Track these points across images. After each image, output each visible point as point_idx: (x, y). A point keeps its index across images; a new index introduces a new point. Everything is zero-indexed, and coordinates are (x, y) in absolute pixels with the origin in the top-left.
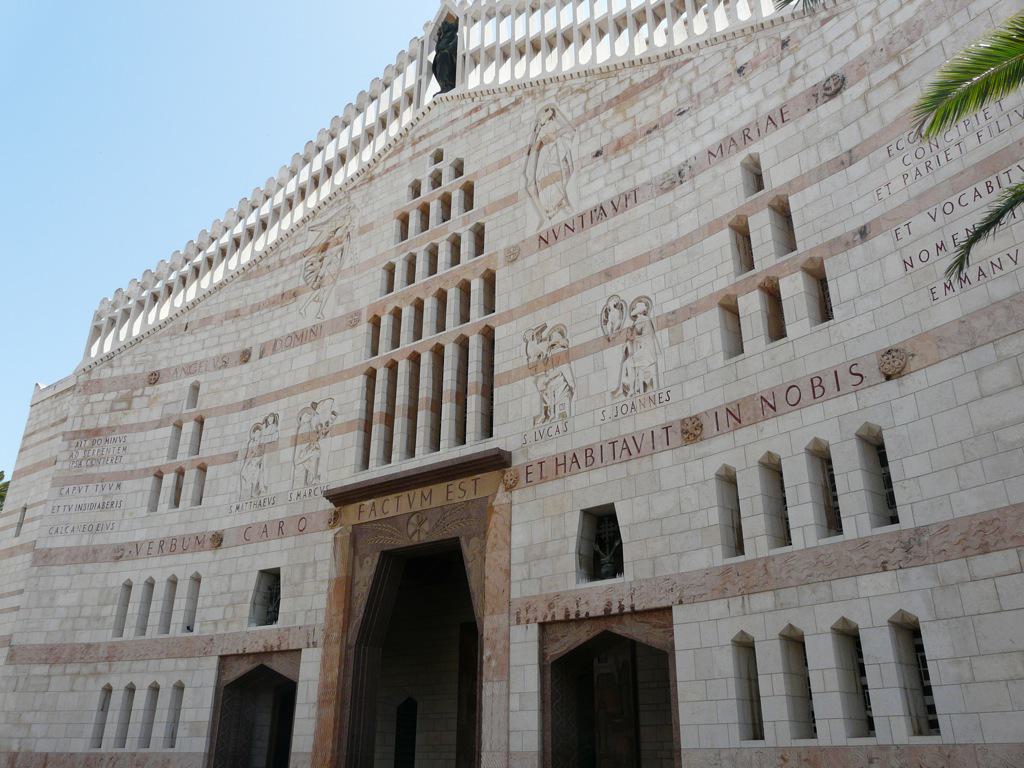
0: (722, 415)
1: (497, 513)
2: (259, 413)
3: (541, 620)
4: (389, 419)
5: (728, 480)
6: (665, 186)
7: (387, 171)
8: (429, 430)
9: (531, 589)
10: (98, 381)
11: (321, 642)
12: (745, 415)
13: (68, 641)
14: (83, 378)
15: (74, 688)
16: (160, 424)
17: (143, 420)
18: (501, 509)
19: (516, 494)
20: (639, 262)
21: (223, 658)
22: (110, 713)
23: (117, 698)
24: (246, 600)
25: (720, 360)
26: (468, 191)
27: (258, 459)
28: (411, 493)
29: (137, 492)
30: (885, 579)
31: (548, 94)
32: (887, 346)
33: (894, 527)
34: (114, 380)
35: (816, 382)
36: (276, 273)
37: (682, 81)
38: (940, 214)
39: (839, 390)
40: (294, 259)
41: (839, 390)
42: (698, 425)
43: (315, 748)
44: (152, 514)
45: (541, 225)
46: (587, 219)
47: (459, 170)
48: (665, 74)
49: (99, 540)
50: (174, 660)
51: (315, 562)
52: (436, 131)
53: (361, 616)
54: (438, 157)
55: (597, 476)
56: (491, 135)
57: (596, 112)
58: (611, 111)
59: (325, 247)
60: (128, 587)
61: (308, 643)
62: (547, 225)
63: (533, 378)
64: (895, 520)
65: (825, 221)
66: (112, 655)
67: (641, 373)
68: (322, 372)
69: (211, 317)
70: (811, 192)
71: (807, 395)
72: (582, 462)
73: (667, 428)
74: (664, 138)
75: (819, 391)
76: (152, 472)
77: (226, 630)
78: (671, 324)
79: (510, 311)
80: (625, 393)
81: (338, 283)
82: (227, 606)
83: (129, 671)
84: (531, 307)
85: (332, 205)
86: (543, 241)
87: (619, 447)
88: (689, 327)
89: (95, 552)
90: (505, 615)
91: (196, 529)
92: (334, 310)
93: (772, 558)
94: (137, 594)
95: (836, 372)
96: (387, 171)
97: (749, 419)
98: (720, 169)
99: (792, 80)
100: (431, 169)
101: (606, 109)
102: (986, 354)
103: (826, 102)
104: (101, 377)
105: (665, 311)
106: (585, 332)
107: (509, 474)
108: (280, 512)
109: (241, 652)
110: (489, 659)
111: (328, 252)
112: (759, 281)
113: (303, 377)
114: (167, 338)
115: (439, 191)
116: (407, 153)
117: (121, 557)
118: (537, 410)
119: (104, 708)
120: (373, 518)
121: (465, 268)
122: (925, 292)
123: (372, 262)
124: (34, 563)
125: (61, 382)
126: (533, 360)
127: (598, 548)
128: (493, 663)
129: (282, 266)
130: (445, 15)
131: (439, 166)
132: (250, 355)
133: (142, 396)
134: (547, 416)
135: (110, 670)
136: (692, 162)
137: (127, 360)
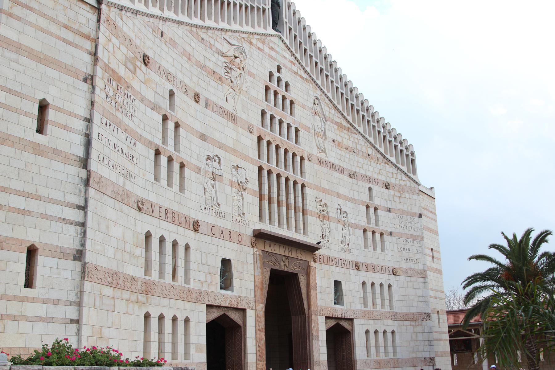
0: (364, 265)
3: (326, 315)
23: (154, 323)
24: (217, 272)
32: (395, 266)
38: (404, 241)
49: (129, 186)
52: (277, 52)
54: (279, 69)
58: (336, 127)
62: (319, 155)
86: (320, 161)
87: (342, 261)
91: (184, 211)
96: (259, 48)
98: (364, 184)
99: (379, 173)
102: (408, 279)
106: (333, 213)
128: (315, 328)
135: (147, 301)
136: (357, 174)
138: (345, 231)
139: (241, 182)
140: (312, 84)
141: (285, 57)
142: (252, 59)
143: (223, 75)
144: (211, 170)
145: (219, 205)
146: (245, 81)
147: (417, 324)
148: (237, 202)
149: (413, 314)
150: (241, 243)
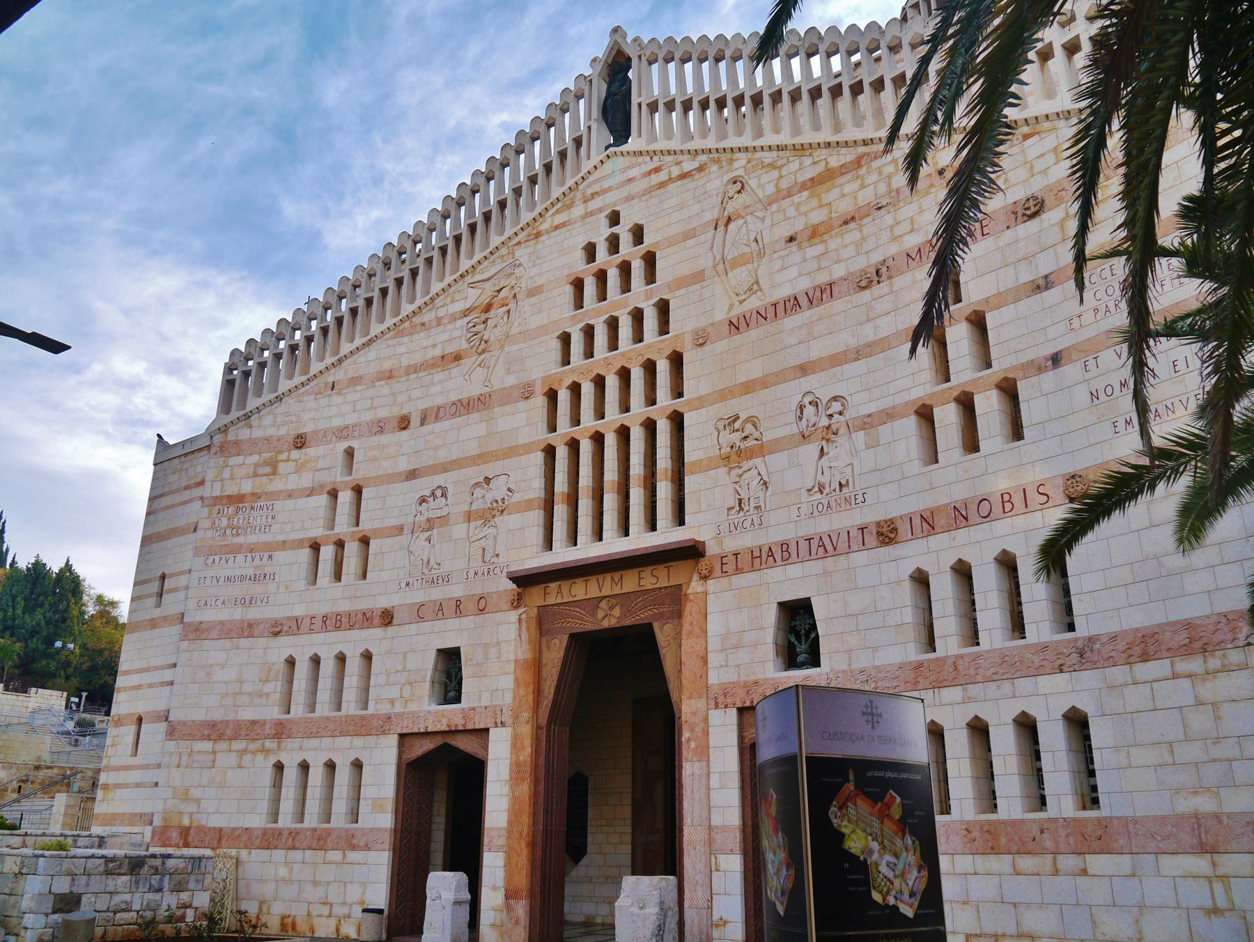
0: (917, 521)
1: (691, 601)
2: (425, 485)
4: (573, 500)
5: (921, 580)
6: (863, 284)
7: (557, 227)
8: (616, 514)
9: (729, 676)
10: (236, 443)
11: (509, 721)
12: (940, 522)
13: (231, 717)
14: (218, 438)
15: (243, 764)
16: (311, 492)
17: (291, 486)
18: (696, 598)
19: (710, 582)
20: (837, 360)
21: (402, 736)
22: (284, 790)
23: (291, 775)
25: (916, 467)
26: (650, 260)
27: (426, 534)
28: (598, 576)
29: (291, 564)
30: (1060, 679)
31: (736, 164)
33: (1070, 635)
34: (254, 442)
35: (1006, 497)
36: (433, 331)
37: (880, 173)
39: (1026, 507)
40: (454, 318)
41: (1026, 507)
42: (893, 529)
43: (510, 822)
44: (310, 588)
45: (731, 307)
46: (780, 308)
47: (638, 234)
48: (863, 164)
49: (253, 614)
50: (349, 738)
51: (499, 643)
53: (551, 696)
54: (614, 219)
55: (794, 570)
56: (673, 202)
57: (789, 194)
59: (488, 308)
60: (291, 662)
61: (496, 723)
62: (738, 310)
63: (727, 469)
64: (1071, 627)
65: (1020, 343)
66: (281, 731)
67: (837, 473)
68: (494, 446)
69: (361, 377)
70: (1007, 312)
71: (997, 509)
72: (778, 556)
73: (862, 529)
74: (861, 231)
75: (1008, 506)
76: (307, 544)
77: (405, 707)
78: (867, 426)
79: (700, 398)
80: (821, 492)
81: (506, 349)
82: (404, 685)
83: (301, 748)
84: (723, 395)
85: (494, 262)
87: (814, 544)
88: (885, 431)
89: (250, 626)
90: (704, 700)
91: (364, 605)
92: (503, 379)
93: (961, 657)
94: (302, 669)
95: (1024, 490)
96: (557, 227)
97: (942, 527)
100: (608, 232)
101: (800, 191)
103: (1024, 222)
104: (239, 438)
105: (862, 413)
106: (779, 427)
107: (703, 563)
108: (457, 591)
109: (422, 730)
110: (688, 740)
111: (492, 314)
112: (955, 394)
113: (473, 449)
114: (312, 397)
115: (617, 259)
116: (578, 210)
117: (280, 632)
118: (732, 502)
119: (277, 784)
120: (559, 600)
121: (649, 346)
122: (1108, 424)
123: (543, 329)
124: (184, 637)
125: (191, 440)
126: (726, 450)
127: (793, 640)
128: (693, 745)
129: (439, 324)
130: (614, 52)
131: (616, 230)
132: (409, 422)
133: (288, 460)
134: (741, 509)
135: (279, 748)
136: (890, 263)
137: (268, 420)
138: (832, 452)
139: (497, 501)
140: (718, 161)
141: (630, 180)
142: (538, 261)
143: (465, 345)
144: (424, 518)
145: (440, 564)
146: (518, 314)
147: (1214, 662)
148: (482, 542)
149: (1188, 625)
150: (487, 610)
